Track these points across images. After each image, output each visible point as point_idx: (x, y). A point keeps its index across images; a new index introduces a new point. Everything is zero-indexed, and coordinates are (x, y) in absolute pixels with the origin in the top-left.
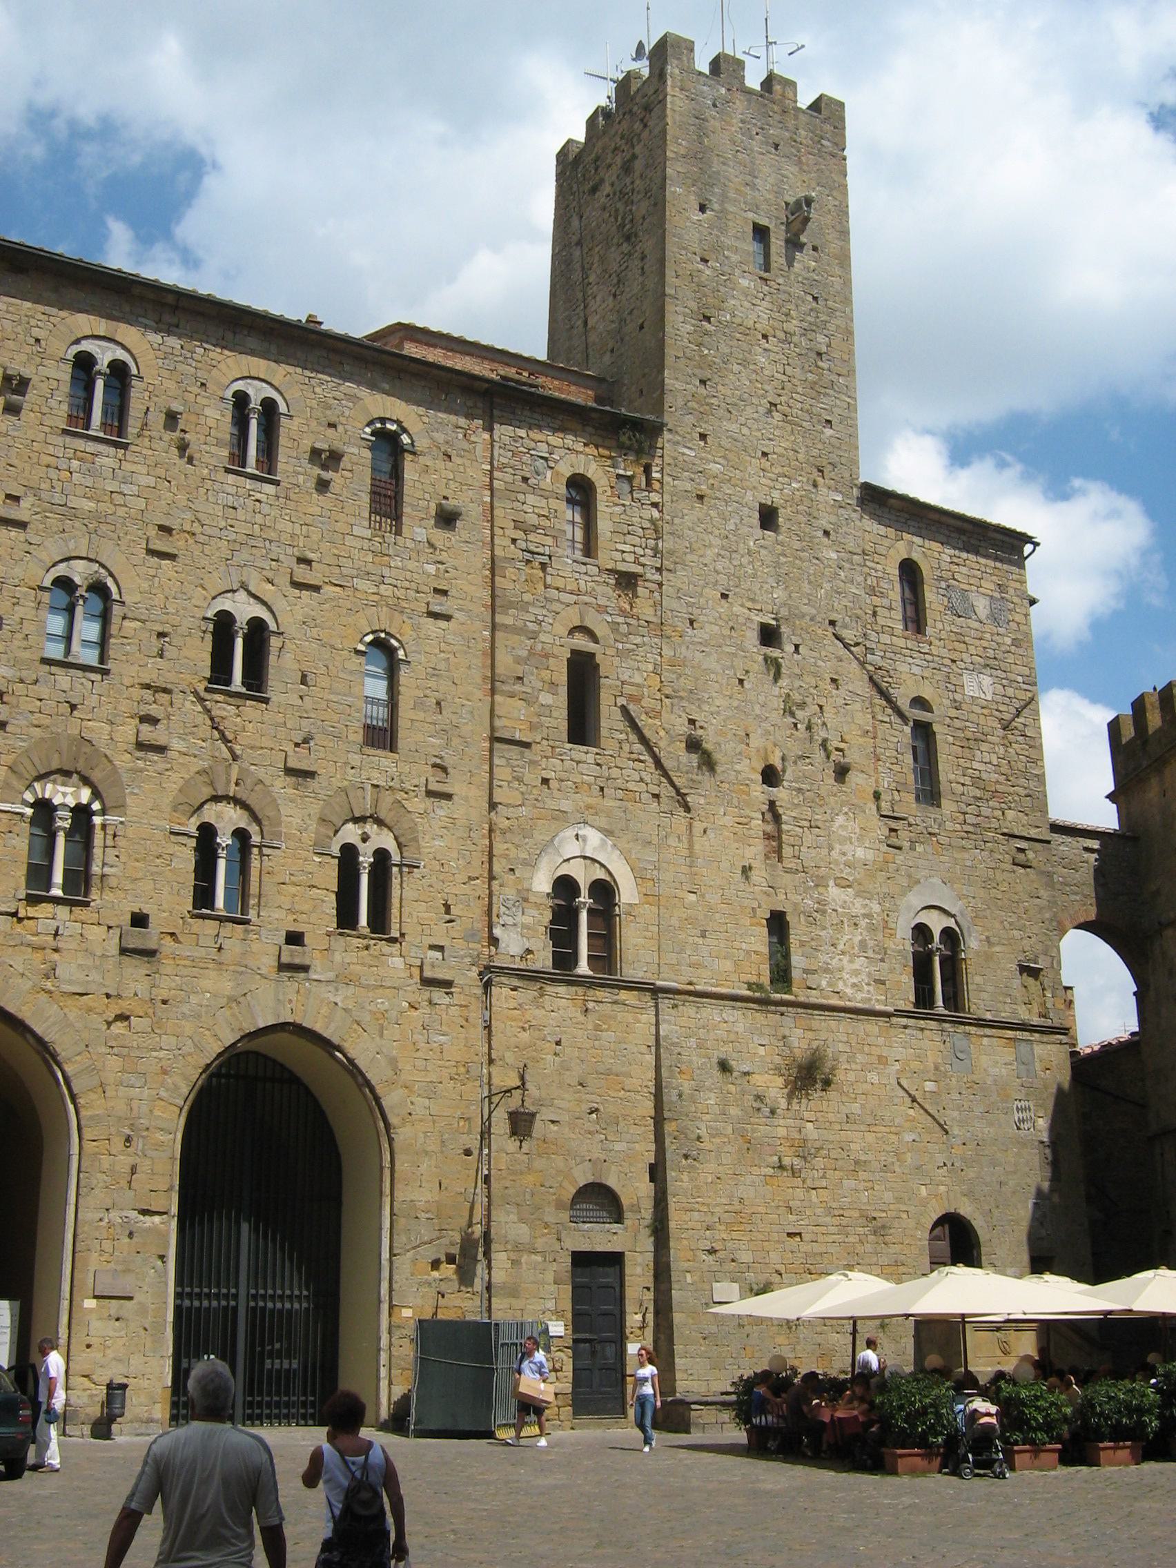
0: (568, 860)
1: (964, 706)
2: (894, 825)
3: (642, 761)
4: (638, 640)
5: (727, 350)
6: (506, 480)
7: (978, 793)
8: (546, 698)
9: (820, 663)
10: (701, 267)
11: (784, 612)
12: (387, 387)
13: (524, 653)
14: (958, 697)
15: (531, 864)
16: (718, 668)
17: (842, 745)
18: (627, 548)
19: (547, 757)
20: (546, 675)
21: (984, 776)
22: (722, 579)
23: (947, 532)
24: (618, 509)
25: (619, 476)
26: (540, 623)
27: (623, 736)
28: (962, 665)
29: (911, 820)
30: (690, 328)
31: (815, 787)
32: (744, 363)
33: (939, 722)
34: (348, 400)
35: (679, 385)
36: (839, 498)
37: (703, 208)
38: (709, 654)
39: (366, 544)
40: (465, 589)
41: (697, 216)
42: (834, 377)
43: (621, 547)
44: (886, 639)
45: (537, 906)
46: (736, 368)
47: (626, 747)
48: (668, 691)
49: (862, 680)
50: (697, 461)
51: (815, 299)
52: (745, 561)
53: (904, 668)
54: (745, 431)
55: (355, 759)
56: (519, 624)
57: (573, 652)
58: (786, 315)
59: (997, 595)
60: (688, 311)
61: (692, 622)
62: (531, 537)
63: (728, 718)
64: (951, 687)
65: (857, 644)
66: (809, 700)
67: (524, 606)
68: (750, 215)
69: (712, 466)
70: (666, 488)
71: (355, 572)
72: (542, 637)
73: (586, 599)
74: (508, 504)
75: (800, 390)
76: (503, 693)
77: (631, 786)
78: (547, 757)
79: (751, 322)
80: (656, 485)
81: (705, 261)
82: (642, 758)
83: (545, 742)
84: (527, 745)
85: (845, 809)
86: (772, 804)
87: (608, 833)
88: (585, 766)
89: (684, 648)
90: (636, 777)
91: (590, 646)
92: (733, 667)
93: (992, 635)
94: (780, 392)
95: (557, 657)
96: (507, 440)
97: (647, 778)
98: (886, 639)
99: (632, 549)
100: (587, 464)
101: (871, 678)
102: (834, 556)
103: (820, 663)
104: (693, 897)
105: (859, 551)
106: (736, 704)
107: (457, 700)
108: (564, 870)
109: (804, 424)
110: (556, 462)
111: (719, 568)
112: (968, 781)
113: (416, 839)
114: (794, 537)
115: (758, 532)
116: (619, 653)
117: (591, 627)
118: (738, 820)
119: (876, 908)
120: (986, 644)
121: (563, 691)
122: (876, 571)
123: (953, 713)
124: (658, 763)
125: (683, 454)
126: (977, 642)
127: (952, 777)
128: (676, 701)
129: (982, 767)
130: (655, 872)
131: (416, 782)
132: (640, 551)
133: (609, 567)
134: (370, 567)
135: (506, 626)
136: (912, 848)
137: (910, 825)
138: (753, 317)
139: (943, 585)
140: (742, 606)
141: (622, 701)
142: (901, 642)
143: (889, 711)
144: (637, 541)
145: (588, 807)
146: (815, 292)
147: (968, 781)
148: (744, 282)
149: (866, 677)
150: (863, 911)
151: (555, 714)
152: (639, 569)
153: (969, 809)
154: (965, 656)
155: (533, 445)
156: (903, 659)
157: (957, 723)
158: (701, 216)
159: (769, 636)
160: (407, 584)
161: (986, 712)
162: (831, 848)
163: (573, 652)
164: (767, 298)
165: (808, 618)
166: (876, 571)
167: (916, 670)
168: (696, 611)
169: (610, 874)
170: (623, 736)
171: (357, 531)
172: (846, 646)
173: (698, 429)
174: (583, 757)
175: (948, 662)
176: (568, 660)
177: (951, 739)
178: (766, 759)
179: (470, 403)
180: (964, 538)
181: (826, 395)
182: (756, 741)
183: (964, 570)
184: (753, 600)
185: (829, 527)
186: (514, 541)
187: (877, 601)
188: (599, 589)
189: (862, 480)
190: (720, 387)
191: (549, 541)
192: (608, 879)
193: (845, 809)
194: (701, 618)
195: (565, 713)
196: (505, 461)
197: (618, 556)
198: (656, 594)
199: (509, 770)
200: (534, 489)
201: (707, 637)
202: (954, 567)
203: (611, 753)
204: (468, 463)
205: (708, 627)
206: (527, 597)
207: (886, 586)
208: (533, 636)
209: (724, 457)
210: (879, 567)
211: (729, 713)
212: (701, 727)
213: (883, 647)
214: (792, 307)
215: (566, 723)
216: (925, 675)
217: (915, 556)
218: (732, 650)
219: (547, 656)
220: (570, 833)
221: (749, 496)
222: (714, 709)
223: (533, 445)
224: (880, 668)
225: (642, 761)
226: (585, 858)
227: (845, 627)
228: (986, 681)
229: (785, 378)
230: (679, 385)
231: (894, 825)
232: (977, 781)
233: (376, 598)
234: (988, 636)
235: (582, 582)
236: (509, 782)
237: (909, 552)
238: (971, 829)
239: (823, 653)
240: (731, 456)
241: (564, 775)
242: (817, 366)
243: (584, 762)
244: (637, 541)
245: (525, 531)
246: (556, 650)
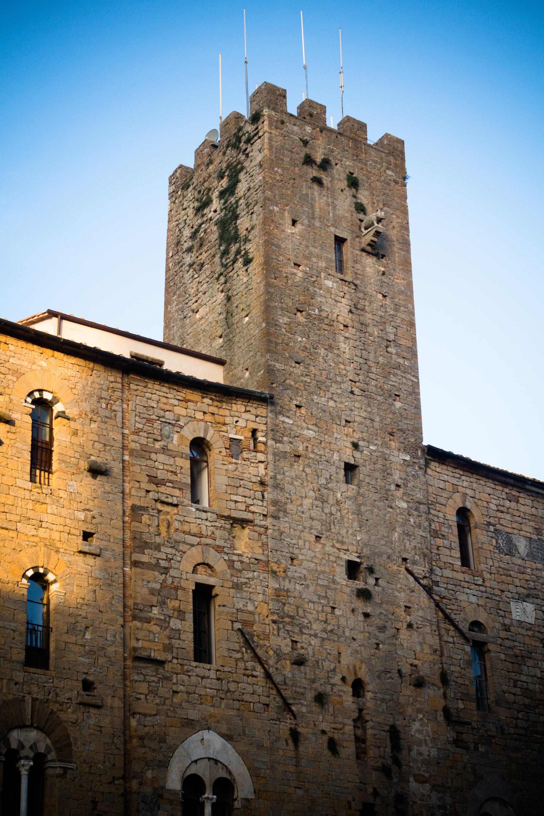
0: (196, 761)
1: (512, 629)
2: (460, 729)
3: (253, 676)
4: (250, 575)
5: (316, 338)
6: (141, 442)
7: (527, 701)
8: (175, 623)
9: (397, 594)
10: (295, 271)
11: (366, 551)
12: (44, 364)
13: (158, 586)
14: (507, 621)
15: (164, 765)
16: (315, 599)
17: (416, 662)
18: (239, 498)
19: (177, 674)
20: (176, 604)
21: (531, 687)
22: (317, 525)
23: (493, 486)
24: (231, 467)
25: (232, 440)
26: (169, 560)
27: (239, 656)
28: (510, 595)
29: (474, 724)
30: (286, 320)
31: (395, 697)
32: (330, 348)
33: (494, 643)
34: (13, 375)
35: (278, 366)
36: (408, 458)
38: (308, 586)
39: (27, 494)
40: (109, 532)
41: (290, 229)
42: (401, 361)
43: (234, 498)
44: (448, 573)
45: (171, 802)
46: (322, 351)
47: (241, 665)
48: (275, 617)
49: (429, 608)
50: (295, 428)
51: (384, 296)
52: (334, 510)
53: (463, 597)
54: (331, 403)
55: (19, 676)
56: (153, 561)
57: (197, 585)
59: (535, 537)
60: (285, 306)
61: (292, 559)
62: (162, 489)
63: (323, 639)
64: (502, 613)
65: (425, 577)
66: (388, 624)
67: (158, 548)
68: (332, 229)
69: (306, 432)
70: (270, 450)
71: (18, 518)
72: (172, 572)
73: (209, 541)
74: (144, 462)
76: (141, 619)
77: (246, 697)
78: (177, 674)
79: (335, 315)
80: (261, 447)
81: (297, 265)
82: (255, 673)
83: (175, 661)
84: (162, 663)
85: (420, 716)
86: (360, 710)
87: (228, 738)
88: (209, 680)
89: (287, 581)
90: (250, 689)
91: (212, 581)
92: (326, 597)
93: (532, 570)
95: (184, 589)
96: (140, 409)
97: (260, 690)
98: (448, 573)
99: (243, 499)
100: (206, 431)
101: (437, 605)
102: (405, 505)
103: (397, 594)
104: (300, 792)
105: (424, 501)
106: (329, 628)
107: (102, 625)
108: (193, 770)
109: (379, 398)
110: (181, 427)
111: (313, 515)
112: (518, 691)
113: (69, 745)
114: (372, 490)
115: (344, 486)
116: (237, 587)
117: (211, 563)
118: (334, 726)
119: (449, 800)
120: (528, 577)
121: (190, 617)
122: (438, 517)
123: (503, 634)
124: (268, 676)
125: (283, 422)
126: (521, 576)
127: (505, 688)
128: (281, 626)
129: (530, 680)
130: (268, 771)
131: (68, 695)
132: (250, 501)
133: (226, 514)
134: (30, 514)
135: (143, 563)
136: (476, 749)
137: (473, 729)
138: (336, 311)
139: (492, 528)
140: (333, 546)
141: (238, 626)
142: (460, 576)
143: (452, 633)
144: (247, 493)
145: (211, 716)
146: (384, 291)
147: (518, 691)
148: (329, 283)
149: (433, 605)
150: (438, 803)
151: (183, 637)
152: (249, 516)
153: (520, 715)
154: (511, 587)
155: (162, 413)
156: (461, 590)
157: (508, 643)
159: (353, 569)
160: (61, 528)
161: (530, 633)
162: (410, 750)
163: (197, 585)
164: (347, 296)
165: (385, 557)
166: (438, 517)
167: (473, 599)
168: (296, 551)
169: (230, 773)
170: (239, 656)
171: (20, 483)
172: (416, 579)
173: (295, 402)
174: (207, 673)
175: (499, 593)
176: (194, 591)
177: (503, 656)
178: (355, 674)
179: (112, 379)
180: (507, 490)
182: (346, 660)
183: (508, 517)
184: (342, 543)
185: (400, 482)
186: (148, 491)
187: (439, 542)
188: (218, 533)
189: (425, 443)
190: (312, 368)
191: (177, 492)
192: (229, 778)
193: (420, 716)
194: (300, 557)
195: (191, 636)
196: (141, 426)
197: (233, 505)
198: (263, 537)
199: (145, 685)
200: (165, 450)
201: (305, 572)
202: (499, 515)
203: (230, 669)
204: (110, 428)
205: (305, 564)
206: (158, 540)
207: (447, 530)
208: (166, 571)
209: (316, 425)
210: (441, 514)
211: (325, 636)
212: (302, 648)
213: (445, 580)
214: (367, 303)
215: (192, 645)
216: (480, 603)
217: (468, 505)
218: (326, 583)
219: (176, 589)
220: (196, 737)
221: (336, 457)
222: (312, 632)
223: (162, 413)
224: (444, 598)
225: (253, 676)
226: (209, 759)
227: (414, 563)
228: (529, 607)
230: (278, 366)
231: (460, 729)
232: (526, 692)
233: (36, 539)
234: (529, 570)
235: (204, 527)
236: (146, 695)
237: (464, 502)
238: (523, 732)
239: (399, 586)
240: (322, 424)
241: (191, 689)
242: (387, 352)
243: (208, 677)
244: (247, 493)
245: (157, 484)
246: (183, 584)
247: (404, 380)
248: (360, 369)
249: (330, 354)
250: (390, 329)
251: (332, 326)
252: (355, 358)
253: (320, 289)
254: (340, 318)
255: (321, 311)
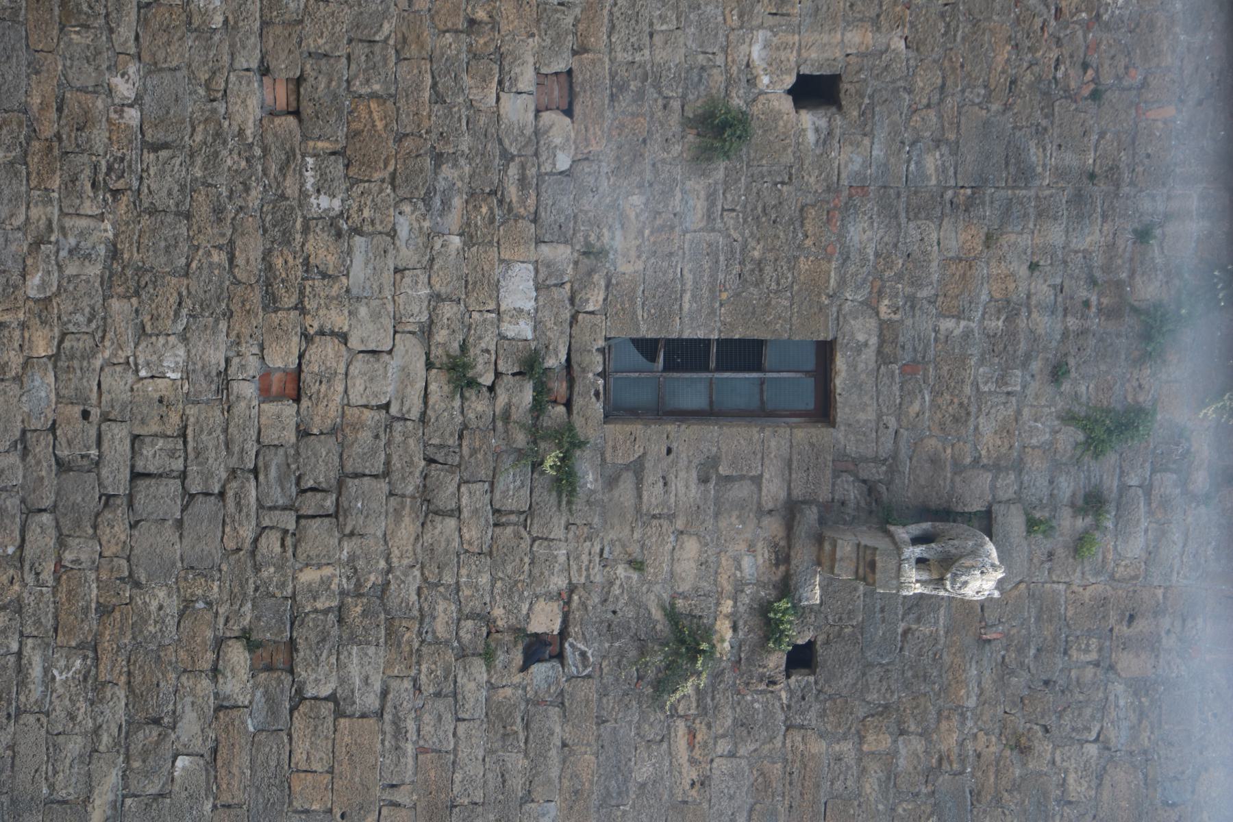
10: (527, 79)
32: (124, 275)
37: (814, 91)
58: (426, 495)
68: (863, 330)
75: (80, 551)
79: (337, 319)
94: (41, 448)
138: (367, 331)
148: (519, 290)
158: (774, 90)
181: (94, 688)
229: (116, 477)
247: (74, 746)
248: (62, 466)
249: (94, 270)
250: (364, 670)
251: (271, 302)
252: (118, 435)
253: (469, 237)
254: (325, 354)
255: (340, 229)
